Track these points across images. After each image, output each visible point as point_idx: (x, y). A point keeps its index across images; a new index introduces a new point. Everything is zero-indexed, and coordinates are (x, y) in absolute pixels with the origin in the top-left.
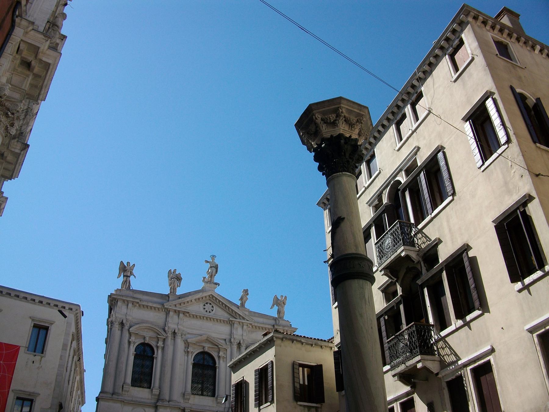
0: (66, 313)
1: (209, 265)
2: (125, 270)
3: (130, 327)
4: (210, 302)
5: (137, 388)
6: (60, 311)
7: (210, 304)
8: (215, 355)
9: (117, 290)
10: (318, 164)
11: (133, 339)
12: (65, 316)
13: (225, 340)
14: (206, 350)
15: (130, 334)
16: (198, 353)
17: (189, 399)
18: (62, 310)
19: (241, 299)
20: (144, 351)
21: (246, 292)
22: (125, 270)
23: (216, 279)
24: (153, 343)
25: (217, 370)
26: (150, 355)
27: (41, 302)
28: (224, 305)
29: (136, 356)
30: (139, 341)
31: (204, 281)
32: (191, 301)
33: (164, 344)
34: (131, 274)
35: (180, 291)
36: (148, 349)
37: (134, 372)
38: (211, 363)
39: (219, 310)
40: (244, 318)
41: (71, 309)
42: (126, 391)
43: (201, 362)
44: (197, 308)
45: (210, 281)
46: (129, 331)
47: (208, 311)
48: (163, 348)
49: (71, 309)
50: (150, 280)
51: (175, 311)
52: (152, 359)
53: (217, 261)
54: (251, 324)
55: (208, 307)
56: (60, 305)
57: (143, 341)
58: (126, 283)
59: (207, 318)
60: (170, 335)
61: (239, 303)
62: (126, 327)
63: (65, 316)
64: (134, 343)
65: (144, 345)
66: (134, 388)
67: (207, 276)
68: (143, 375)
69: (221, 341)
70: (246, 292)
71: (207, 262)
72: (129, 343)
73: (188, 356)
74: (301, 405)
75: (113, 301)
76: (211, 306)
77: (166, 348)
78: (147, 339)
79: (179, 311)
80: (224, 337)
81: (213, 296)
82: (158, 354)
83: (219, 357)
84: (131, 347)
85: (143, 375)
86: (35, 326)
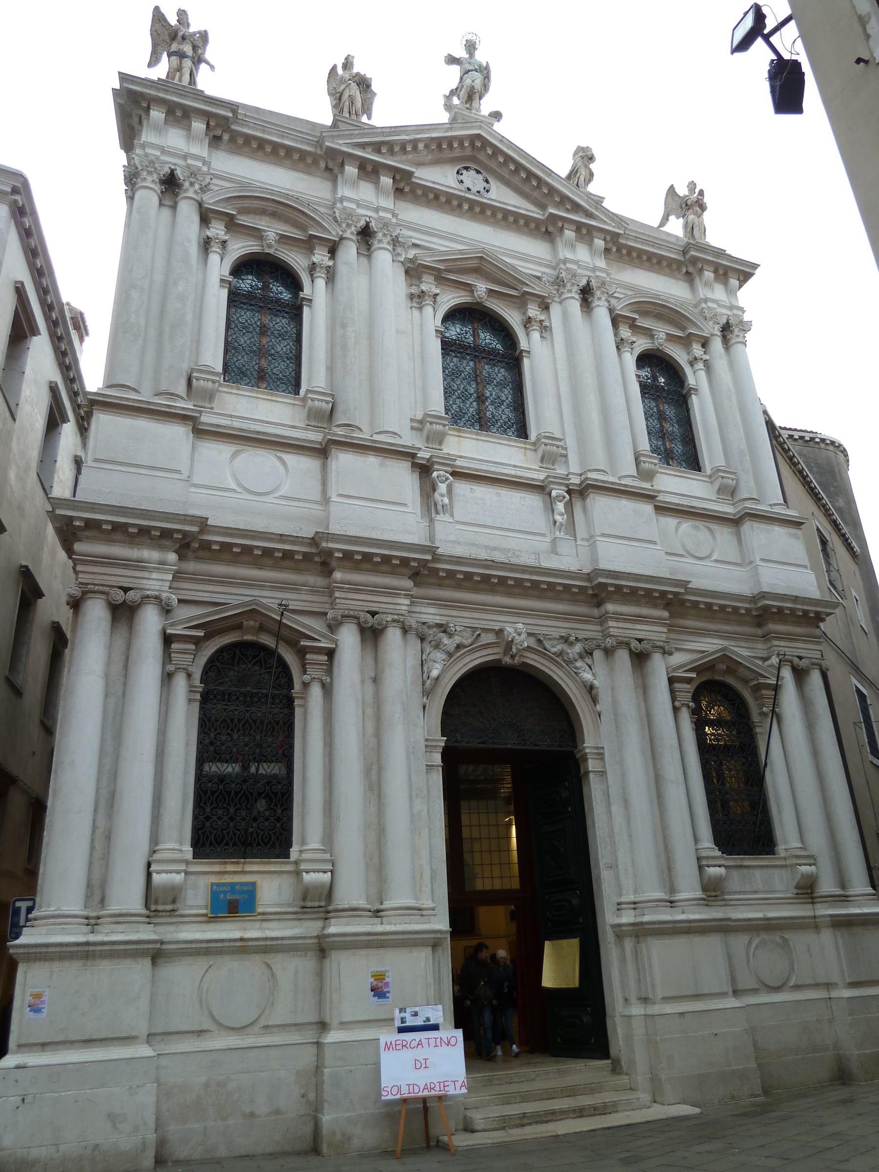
7: (478, 172)
8: (513, 317)
25: (526, 362)
32: (415, 148)
40: (589, 215)
47: (474, 190)
52: (295, 311)
53: (481, 56)
57: (256, 249)
72: (206, 245)
73: (420, 308)
76: (480, 177)
81: (486, 143)
82: (316, 290)
83: (528, 323)
84: (214, 258)
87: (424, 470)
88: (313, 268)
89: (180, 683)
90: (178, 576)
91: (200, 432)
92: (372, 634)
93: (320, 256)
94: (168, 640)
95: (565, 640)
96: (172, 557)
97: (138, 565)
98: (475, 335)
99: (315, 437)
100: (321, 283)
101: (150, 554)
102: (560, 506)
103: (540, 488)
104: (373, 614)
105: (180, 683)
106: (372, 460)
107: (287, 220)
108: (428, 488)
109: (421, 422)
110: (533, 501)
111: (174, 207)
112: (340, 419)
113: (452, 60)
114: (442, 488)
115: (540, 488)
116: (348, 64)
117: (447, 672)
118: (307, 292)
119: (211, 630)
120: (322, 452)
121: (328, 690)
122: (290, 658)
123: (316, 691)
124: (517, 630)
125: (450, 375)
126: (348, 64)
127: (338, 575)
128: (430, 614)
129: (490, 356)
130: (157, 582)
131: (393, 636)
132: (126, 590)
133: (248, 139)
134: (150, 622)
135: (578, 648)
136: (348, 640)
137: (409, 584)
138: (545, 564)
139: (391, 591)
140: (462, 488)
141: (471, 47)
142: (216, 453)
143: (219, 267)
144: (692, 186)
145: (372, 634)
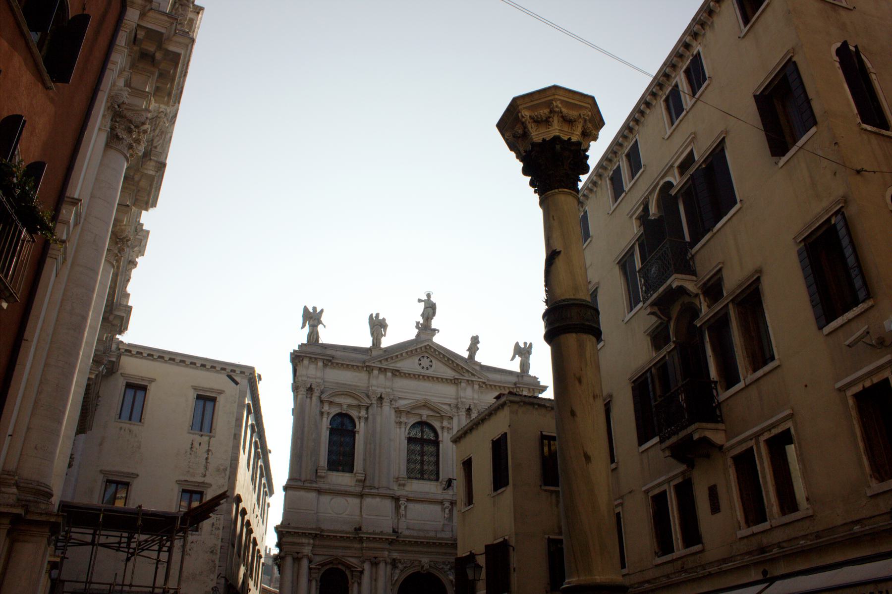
0: (237, 379)
1: (422, 305)
2: (312, 318)
3: (322, 392)
4: (426, 355)
5: (335, 473)
6: (230, 377)
8: (437, 425)
9: (301, 346)
10: (529, 178)
11: (326, 408)
12: (237, 383)
13: (450, 405)
14: (424, 418)
15: (322, 402)
16: (414, 424)
17: (404, 485)
18: (232, 374)
19: (469, 349)
20: (342, 424)
21: (475, 341)
22: (312, 318)
23: (434, 324)
24: (354, 413)
25: (441, 445)
26: (350, 428)
27: (203, 366)
28: (447, 357)
29: (332, 431)
30: (335, 410)
31: (417, 327)
33: (367, 413)
34: (320, 322)
35: (385, 343)
36: (346, 421)
37: (330, 452)
38: (432, 437)
39: (440, 364)
41: (242, 372)
42: (321, 477)
43: (419, 435)
44: (410, 365)
45: (426, 329)
46: (320, 397)
48: (366, 419)
49: (242, 372)
50: (345, 331)
51: (380, 369)
52: (353, 434)
54: (484, 383)
55: (425, 362)
56: (229, 369)
58: (313, 336)
59: (424, 376)
60: (374, 401)
61: (466, 355)
62: (316, 394)
63: (237, 383)
64: (328, 414)
65: (340, 415)
66: (331, 473)
67: (421, 321)
68: (342, 455)
69: (444, 407)
70: (475, 341)
71: (420, 301)
72: (322, 414)
74: (546, 491)
75: (297, 358)
77: (370, 417)
78: (345, 407)
79: (385, 369)
80: (448, 401)
81: (430, 347)
82: (361, 427)
83: (443, 428)
84: (325, 419)
85: (342, 455)
86: (199, 397)
87: (396, 499)
88: (359, 418)
89: (314, 583)
90: (314, 546)
91: (320, 491)
92: (375, 564)
93: (363, 413)
94: (310, 569)
95: (444, 563)
96: (312, 541)
97: (302, 544)
98: (422, 432)
99: (358, 489)
100: (362, 424)
101: (304, 540)
102: (447, 511)
103: (441, 503)
104: (376, 558)
105: (314, 583)
106: (378, 500)
107: (351, 396)
108: (398, 507)
109: (397, 478)
110: (438, 508)
111: (311, 398)
112: (367, 483)
113: (420, 301)
114: (403, 507)
115: (441, 503)
116: (377, 315)
117: (399, 576)
118: (357, 428)
119: (323, 565)
120: (361, 496)
121: (360, 584)
122: (348, 573)
123: (356, 585)
124: (425, 560)
125: (410, 452)
126: (377, 315)
127: (364, 545)
128: (395, 555)
129: (429, 442)
130: (307, 550)
131: (382, 565)
132: (298, 553)
133: (337, 364)
134: (305, 563)
135: (449, 567)
136: (367, 566)
137: (387, 546)
138: (439, 536)
139: (383, 549)
140: (411, 506)
141: (429, 296)
142: (325, 499)
143: (326, 422)
144: (525, 344)
145: (375, 564)
